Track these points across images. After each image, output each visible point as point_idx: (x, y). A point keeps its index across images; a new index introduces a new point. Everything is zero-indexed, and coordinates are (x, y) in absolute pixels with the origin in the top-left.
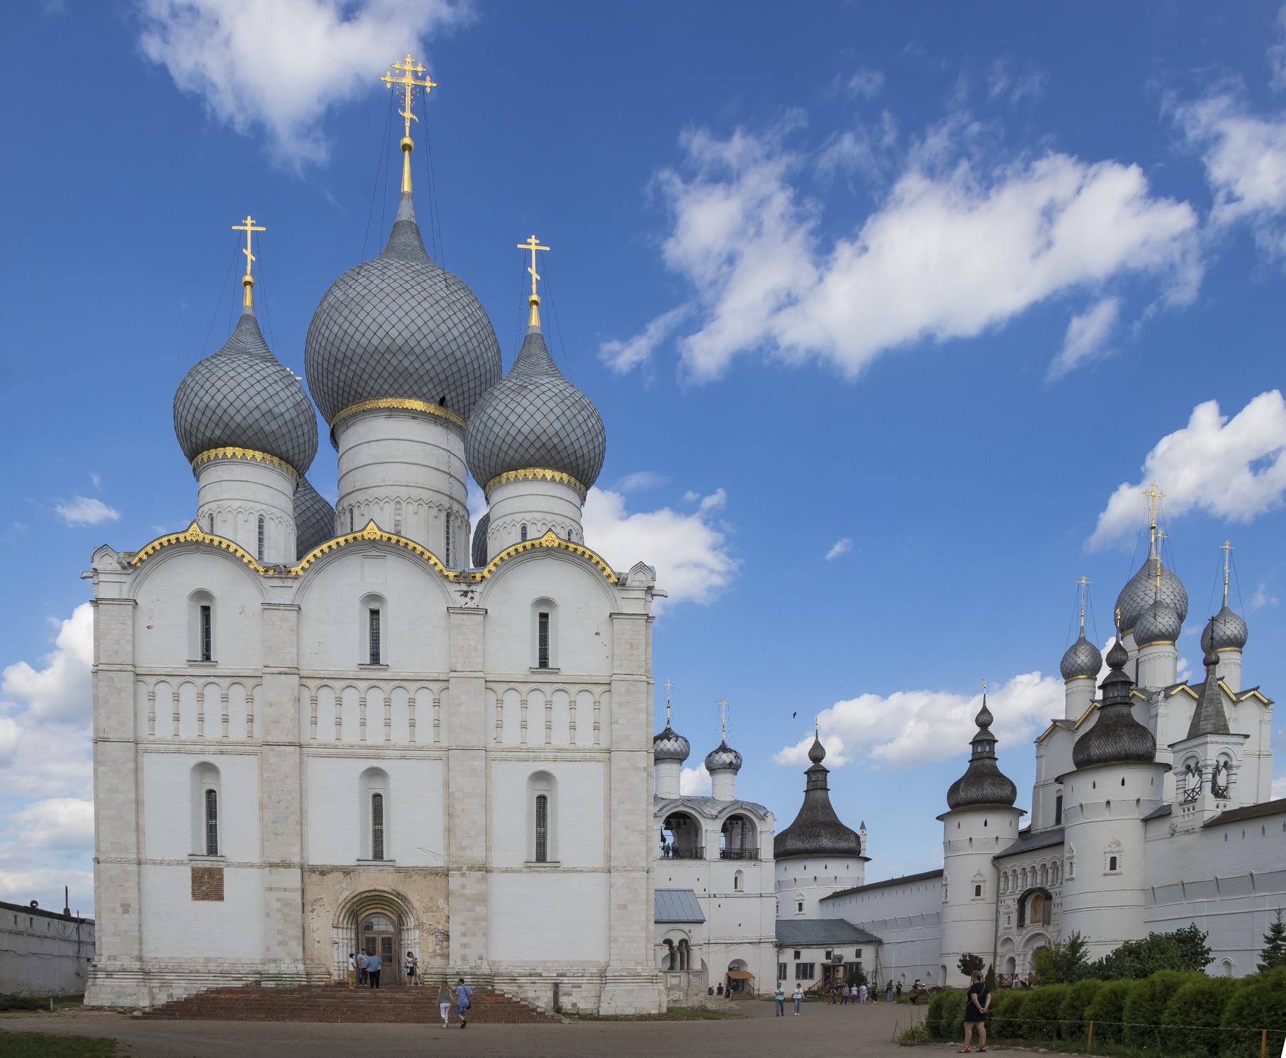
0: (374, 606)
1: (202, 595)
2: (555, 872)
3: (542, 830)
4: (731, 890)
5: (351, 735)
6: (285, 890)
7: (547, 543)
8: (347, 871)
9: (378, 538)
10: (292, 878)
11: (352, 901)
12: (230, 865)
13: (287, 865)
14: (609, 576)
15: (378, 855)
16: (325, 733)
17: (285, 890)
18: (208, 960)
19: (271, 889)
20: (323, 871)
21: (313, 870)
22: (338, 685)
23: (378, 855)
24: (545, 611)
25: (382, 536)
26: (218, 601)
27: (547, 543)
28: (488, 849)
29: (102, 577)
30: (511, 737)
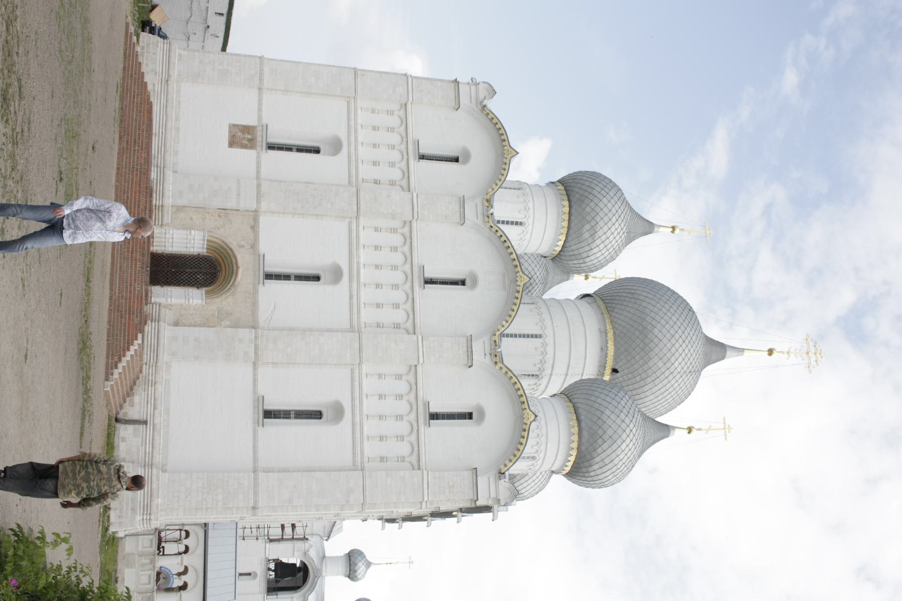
0: (467, 282)
1: (467, 156)
2: (254, 423)
3: (292, 415)
4: (241, 570)
5: (365, 256)
6: (238, 195)
7: (526, 414)
8: (254, 246)
9: (518, 283)
10: (248, 203)
11: (228, 250)
12: (258, 153)
13: (258, 202)
14: (505, 466)
15: (269, 276)
16: (366, 236)
17: (238, 195)
18: (178, 130)
19: (238, 182)
20: (255, 228)
21: (256, 219)
22: (406, 249)
23: (269, 276)
24: (474, 416)
25: (519, 286)
26: (463, 166)
27: (526, 414)
28: (275, 364)
29: (473, 88)
30: (369, 385)
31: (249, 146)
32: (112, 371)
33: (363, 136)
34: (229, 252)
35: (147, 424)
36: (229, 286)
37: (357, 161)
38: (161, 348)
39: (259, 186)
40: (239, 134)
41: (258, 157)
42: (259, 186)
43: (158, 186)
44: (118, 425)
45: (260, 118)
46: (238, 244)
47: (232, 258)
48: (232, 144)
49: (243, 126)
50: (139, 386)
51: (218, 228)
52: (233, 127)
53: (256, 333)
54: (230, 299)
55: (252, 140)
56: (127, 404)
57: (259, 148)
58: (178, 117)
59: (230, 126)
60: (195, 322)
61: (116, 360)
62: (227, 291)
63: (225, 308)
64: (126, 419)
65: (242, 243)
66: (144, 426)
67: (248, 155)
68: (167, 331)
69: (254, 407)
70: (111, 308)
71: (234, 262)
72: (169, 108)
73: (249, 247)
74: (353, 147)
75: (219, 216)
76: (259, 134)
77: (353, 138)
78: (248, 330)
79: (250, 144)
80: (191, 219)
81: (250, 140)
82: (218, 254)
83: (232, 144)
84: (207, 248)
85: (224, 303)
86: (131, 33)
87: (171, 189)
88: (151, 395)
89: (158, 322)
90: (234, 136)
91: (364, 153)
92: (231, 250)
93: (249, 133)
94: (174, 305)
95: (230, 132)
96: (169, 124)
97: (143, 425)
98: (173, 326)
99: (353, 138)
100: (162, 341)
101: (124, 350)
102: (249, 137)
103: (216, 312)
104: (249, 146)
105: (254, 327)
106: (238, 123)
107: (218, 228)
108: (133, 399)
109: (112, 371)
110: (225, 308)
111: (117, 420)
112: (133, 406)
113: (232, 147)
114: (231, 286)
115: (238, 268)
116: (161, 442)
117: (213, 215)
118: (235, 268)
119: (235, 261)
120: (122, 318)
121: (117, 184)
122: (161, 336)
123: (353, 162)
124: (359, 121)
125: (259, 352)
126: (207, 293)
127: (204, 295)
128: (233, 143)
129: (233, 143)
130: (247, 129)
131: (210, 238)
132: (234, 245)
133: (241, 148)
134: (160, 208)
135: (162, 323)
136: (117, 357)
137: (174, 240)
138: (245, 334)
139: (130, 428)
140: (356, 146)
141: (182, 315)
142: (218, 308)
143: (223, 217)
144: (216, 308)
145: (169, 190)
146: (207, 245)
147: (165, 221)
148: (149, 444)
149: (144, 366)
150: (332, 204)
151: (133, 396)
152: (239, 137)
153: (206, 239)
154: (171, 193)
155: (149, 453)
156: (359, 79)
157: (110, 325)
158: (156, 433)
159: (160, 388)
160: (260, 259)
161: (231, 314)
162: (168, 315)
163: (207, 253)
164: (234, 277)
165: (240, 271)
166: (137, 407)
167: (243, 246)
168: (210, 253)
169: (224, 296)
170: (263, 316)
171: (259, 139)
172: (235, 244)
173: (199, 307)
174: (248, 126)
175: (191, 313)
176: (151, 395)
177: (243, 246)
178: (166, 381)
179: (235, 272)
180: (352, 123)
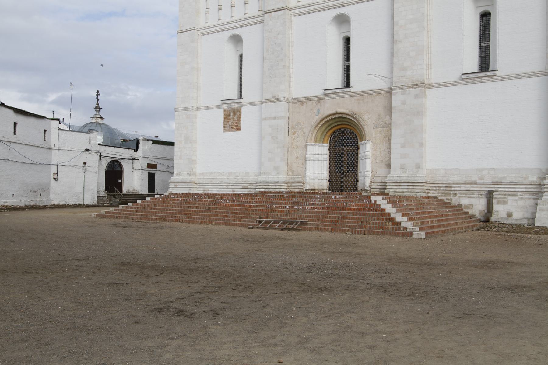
6: (275, 118)
8: (318, 100)
10: (281, 109)
12: (243, 105)
17: (275, 118)
18: (230, 173)
31: (238, 114)
32: (402, 229)
33: (225, 16)
34: (323, 122)
35: (493, 191)
36: (353, 120)
37: (245, 19)
38: (411, 179)
39: (267, 101)
40: (230, 123)
41: (246, 105)
42: (267, 101)
43: (270, 187)
44: (493, 220)
45: (218, 107)
46: (316, 115)
47: (329, 119)
48: (238, 128)
49: (224, 120)
50: (451, 200)
51: (304, 133)
52: (225, 129)
53: (396, 89)
54: (365, 117)
55: (234, 112)
56: (470, 212)
57: (240, 105)
58: (221, 174)
59: (225, 131)
60: (388, 149)
61: (390, 223)
62: (357, 121)
63: (374, 122)
64: (486, 211)
65: (316, 111)
66: (494, 193)
67: (245, 112)
68: (396, 174)
69: (474, 83)
70: (330, 230)
71: (332, 117)
72: (214, 181)
73: (319, 104)
74: (235, 25)
75: (294, 134)
76: (229, 106)
77: (227, 26)
78: (393, 97)
79: (237, 112)
80: (297, 158)
81: (234, 114)
82: (327, 133)
83: (238, 128)
84: (323, 142)
85: (369, 123)
86: (115, 210)
87: (272, 177)
88: (460, 187)
89: (387, 182)
90: (232, 127)
91: (238, 14)
92: (322, 120)
93: (230, 115)
94: (372, 169)
95: (229, 131)
96: (226, 180)
97: (493, 195)
98: (390, 169)
99: (227, 26)
100: (405, 179)
101: (382, 215)
102: (232, 114)
103: (378, 129)
104: (238, 114)
105: (390, 92)
106: (222, 124)
107: (304, 133)
108: (465, 205)
109: (402, 229)
110: (374, 122)
111: (487, 220)
112: (472, 205)
113: (241, 128)
114: (354, 118)
115: (337, 113)
116: (514, 176)
117: (294, 140)
118: (338, 116)
119: (331, 116)
120: (346, 218)
121: (214, 223)
122: (399, 179)
123: (245, 23)
124: (216, 23)
125: (415, 83)
126: (361, 140)
127: (364, 142)
128: (237, 128)
129: (237, 128)
130: (227, 117)
131: (313, 141)
132: (317, 118)
133: (241, 120)
134: (289, 185)
135: (387, 180)
136: (387, 223)
137: (316, 172)
138: (397, 99)
139: (496, 207)
140: (234, 22)
141: (382, 161)
142: (374, 128)
143: (295, 131)
144: (374, 130)
145: (273, 178)
146: (319, 143)
147: (300, 180)
148: (515, 188)
149: (430, 195)
150: (279, 34)
151: (462, 205)
152: (233, 122)
153: (313, 144)
154: (275, 176)
155: (526, 188)
156: (184, 28)
157: (348, 231)
158: (504, 181)
159: (455, 179)
160: (329, 93)
161: (379, 116)
162: (381, 173)
163: (327, 143)
164: (345, 116)
165: (339, 110)
166: (473, 201)
167: (319, 110)
168: (328, 140)
169: (362, 123)
170: (382, 84)
171: (233, 106)
172: (317, 117)
173: (373, 146)
174: (224, 116)
175: (379, 153)
176: (460, 187)
177: (319, 110)
178: (446, 173)
179: (340, 116)
180: (217, 28)
